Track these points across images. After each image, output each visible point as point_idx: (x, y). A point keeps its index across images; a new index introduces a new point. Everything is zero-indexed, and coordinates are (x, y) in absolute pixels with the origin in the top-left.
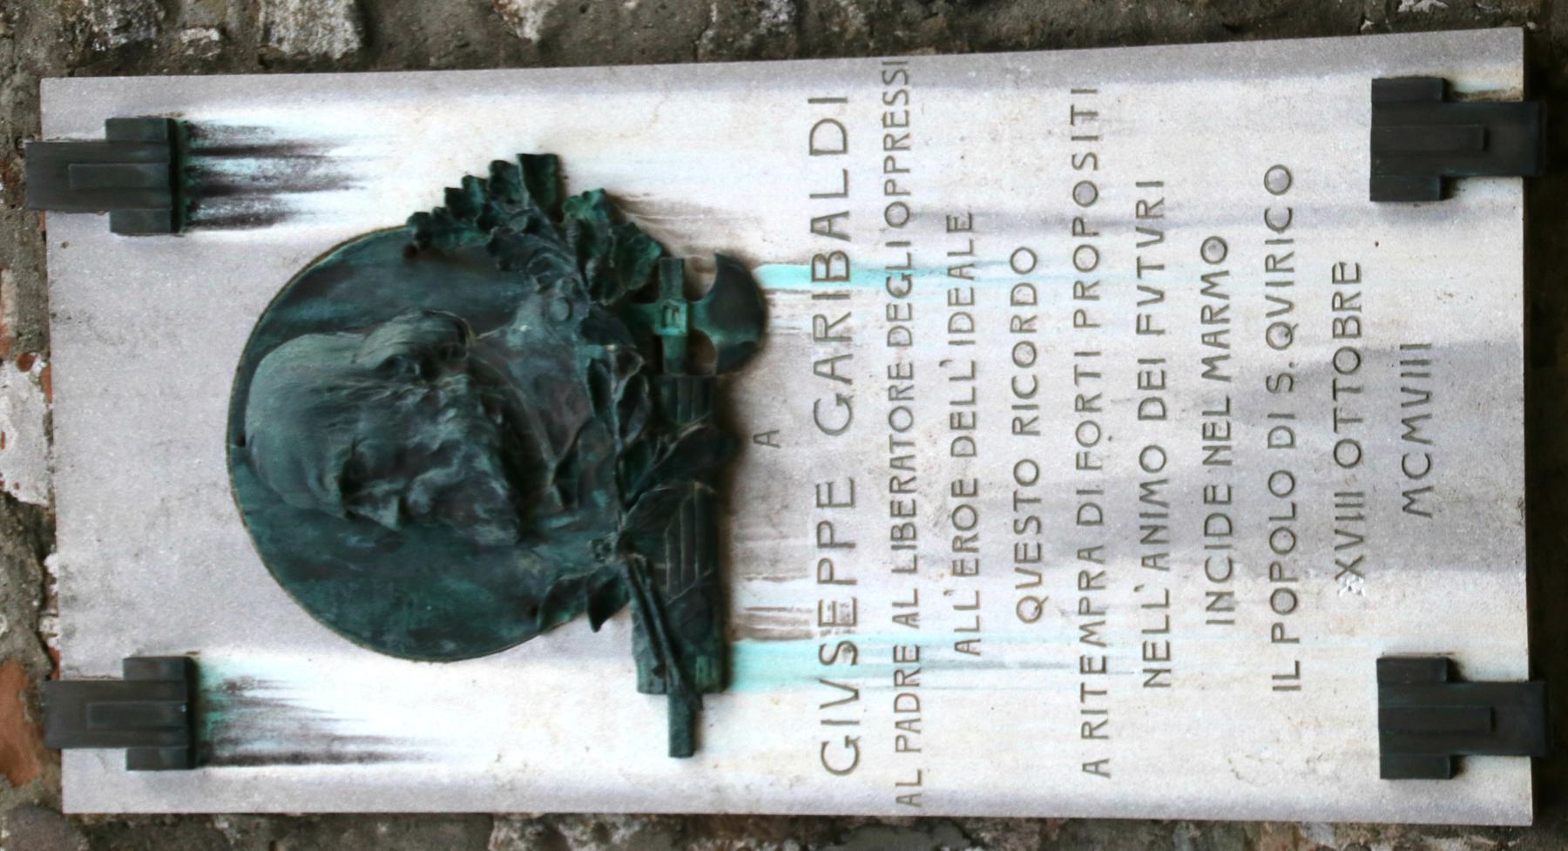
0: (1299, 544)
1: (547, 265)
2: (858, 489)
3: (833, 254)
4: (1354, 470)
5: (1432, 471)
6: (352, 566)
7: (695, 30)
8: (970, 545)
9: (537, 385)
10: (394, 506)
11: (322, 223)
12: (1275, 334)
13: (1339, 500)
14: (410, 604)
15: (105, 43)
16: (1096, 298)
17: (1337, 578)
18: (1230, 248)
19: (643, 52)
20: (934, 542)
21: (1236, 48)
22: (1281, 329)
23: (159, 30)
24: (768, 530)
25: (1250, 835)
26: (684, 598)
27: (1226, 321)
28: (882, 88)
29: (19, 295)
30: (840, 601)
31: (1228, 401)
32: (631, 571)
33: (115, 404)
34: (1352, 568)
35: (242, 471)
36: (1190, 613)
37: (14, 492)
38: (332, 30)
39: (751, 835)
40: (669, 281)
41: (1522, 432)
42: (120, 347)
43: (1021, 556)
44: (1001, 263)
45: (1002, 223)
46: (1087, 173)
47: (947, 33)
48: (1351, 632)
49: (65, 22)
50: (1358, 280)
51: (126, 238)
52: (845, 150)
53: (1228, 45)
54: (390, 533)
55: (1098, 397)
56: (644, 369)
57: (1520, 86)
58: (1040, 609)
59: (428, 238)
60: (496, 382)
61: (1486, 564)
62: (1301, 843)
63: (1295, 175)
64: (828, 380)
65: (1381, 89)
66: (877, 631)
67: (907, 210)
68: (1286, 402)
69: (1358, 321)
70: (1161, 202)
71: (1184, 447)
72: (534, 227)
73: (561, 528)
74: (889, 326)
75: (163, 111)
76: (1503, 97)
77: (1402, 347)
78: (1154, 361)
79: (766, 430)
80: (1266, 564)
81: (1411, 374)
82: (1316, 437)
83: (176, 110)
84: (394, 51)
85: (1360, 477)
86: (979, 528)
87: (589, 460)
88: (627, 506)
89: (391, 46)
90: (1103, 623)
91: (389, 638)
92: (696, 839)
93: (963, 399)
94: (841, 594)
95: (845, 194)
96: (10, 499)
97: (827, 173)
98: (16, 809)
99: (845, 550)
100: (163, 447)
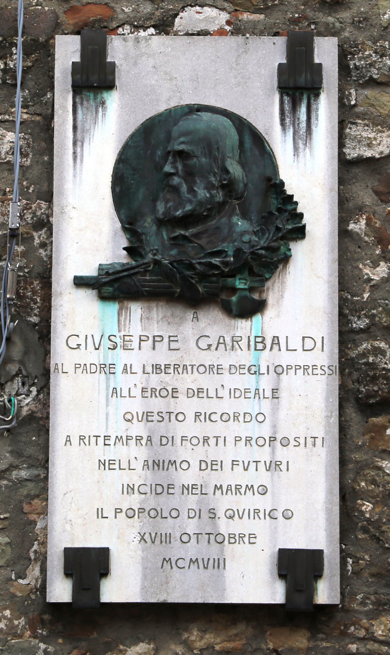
0: (152, 519)
1: (263, 234)
2: (175, 352)
3: (265, 344)
4: (179, 540)
5: (178, 569)
6: (149, 152)
7: (351, 291)
8: (153, 395)
9: (218, 228)
10: (172, 171)
11: (281, 145)
12: (231, 512)
13: (168, 534)
14: (134, 174)
15: (351, 60)
16: (246, 445)
17: (139, 533)
18: (263, 496)
19: (343, 270)
20: (155, 381)
21: (337, 499)
22: (233, 514)
23: (355, 81)
24: (160, 316)
25: (41, 497)
26: (135, 284)
27: (236, 494)
28: (327, 365)
29: (255, 21)
30: (133, 343)
31: (206, 494)
32: (146, 263)
33: (213, 61)
34: (143, 538)
35: (187, 110)
36: (127, 478)
37: (179, 16)
38: (354, 149)
39: (42, 304)
40: (257, 281)
41: (192, 602)
42: (235, 63)
43: (149, 414)
44: (260, 409)
45: (275, 410)
46: (293, 443)
47: (346, 389)
48: (118, 538)
49: (359, 44)
50: (250, 543)
51: (277, 68)
52: (304, 350)
53: (338, 496)
54: (162, 168)
55: (209, 445)
56: (223, 271)
57: (318, 603)
58: (129, 421)
59: (275, 187)
60: (219, 212)
61: (143, 588)
62: (38, 516)
63: (289, 520)
64: (217, 341)
65: (320, 552)
66: (121, 358)
67: (281, 374)
68: (205, 516)
69: (235, 543)
70: (281, 470)
71: (189, 477)
72: (278, 229)
73: (163, 236)
74: (237, 366)
75: (325, 85)
76: (315, 597)
77: (224, 559)
78: (221, 467)
79: (199, 317)
80: (144, 506)
81: (214, 562)
82: (192, 527)
83: (325, 90)
84: (345, 172)
85: (177, 542)
86: (159, 398)
87: (190, 248)
88: (171, 263)
89: (348, 171)
90: (123, 445)
91: (121, 165)
92: (41, 282)
93: (209, 393)
94: (135, 344)
95: (287, 350)
96: (176, 15)
97: (296, 343)
98: (56, 13)
99: (152, 347)
100: (196, 79)
